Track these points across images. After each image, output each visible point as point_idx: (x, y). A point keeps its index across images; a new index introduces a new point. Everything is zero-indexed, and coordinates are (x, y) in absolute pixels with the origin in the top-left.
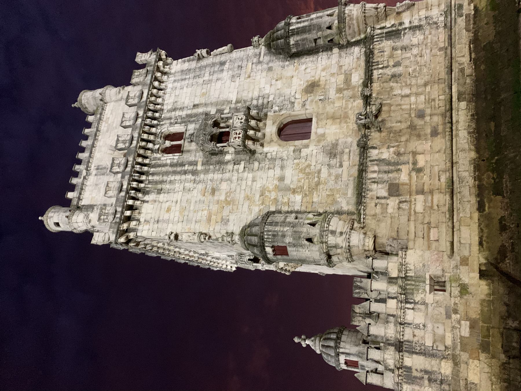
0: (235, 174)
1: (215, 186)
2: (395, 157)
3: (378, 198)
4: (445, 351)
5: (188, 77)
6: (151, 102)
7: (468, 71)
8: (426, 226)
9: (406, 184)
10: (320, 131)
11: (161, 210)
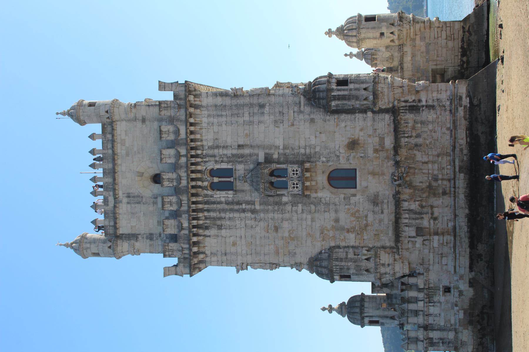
0: (295, 214)
1: (277, 224)
3: (409, 237)
5: (224, 113)
7: (465, 151)
9: (428, 228)
10: (364, 184)
11: (226, 244)
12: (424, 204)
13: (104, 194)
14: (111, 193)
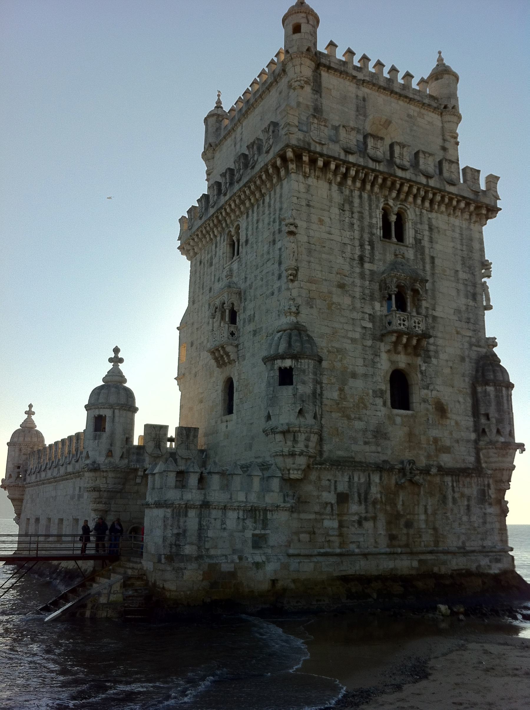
1: (347, 288)
2: (372, 499)
3: (336, 482)
4: (205, 548)
5: (465, 248)
6: (443, 197)
8: (311, 529)
10: (398, 420)
11: (321, 209)
12: (378, 506)
13: (366, 70)
14: (367, 78)
